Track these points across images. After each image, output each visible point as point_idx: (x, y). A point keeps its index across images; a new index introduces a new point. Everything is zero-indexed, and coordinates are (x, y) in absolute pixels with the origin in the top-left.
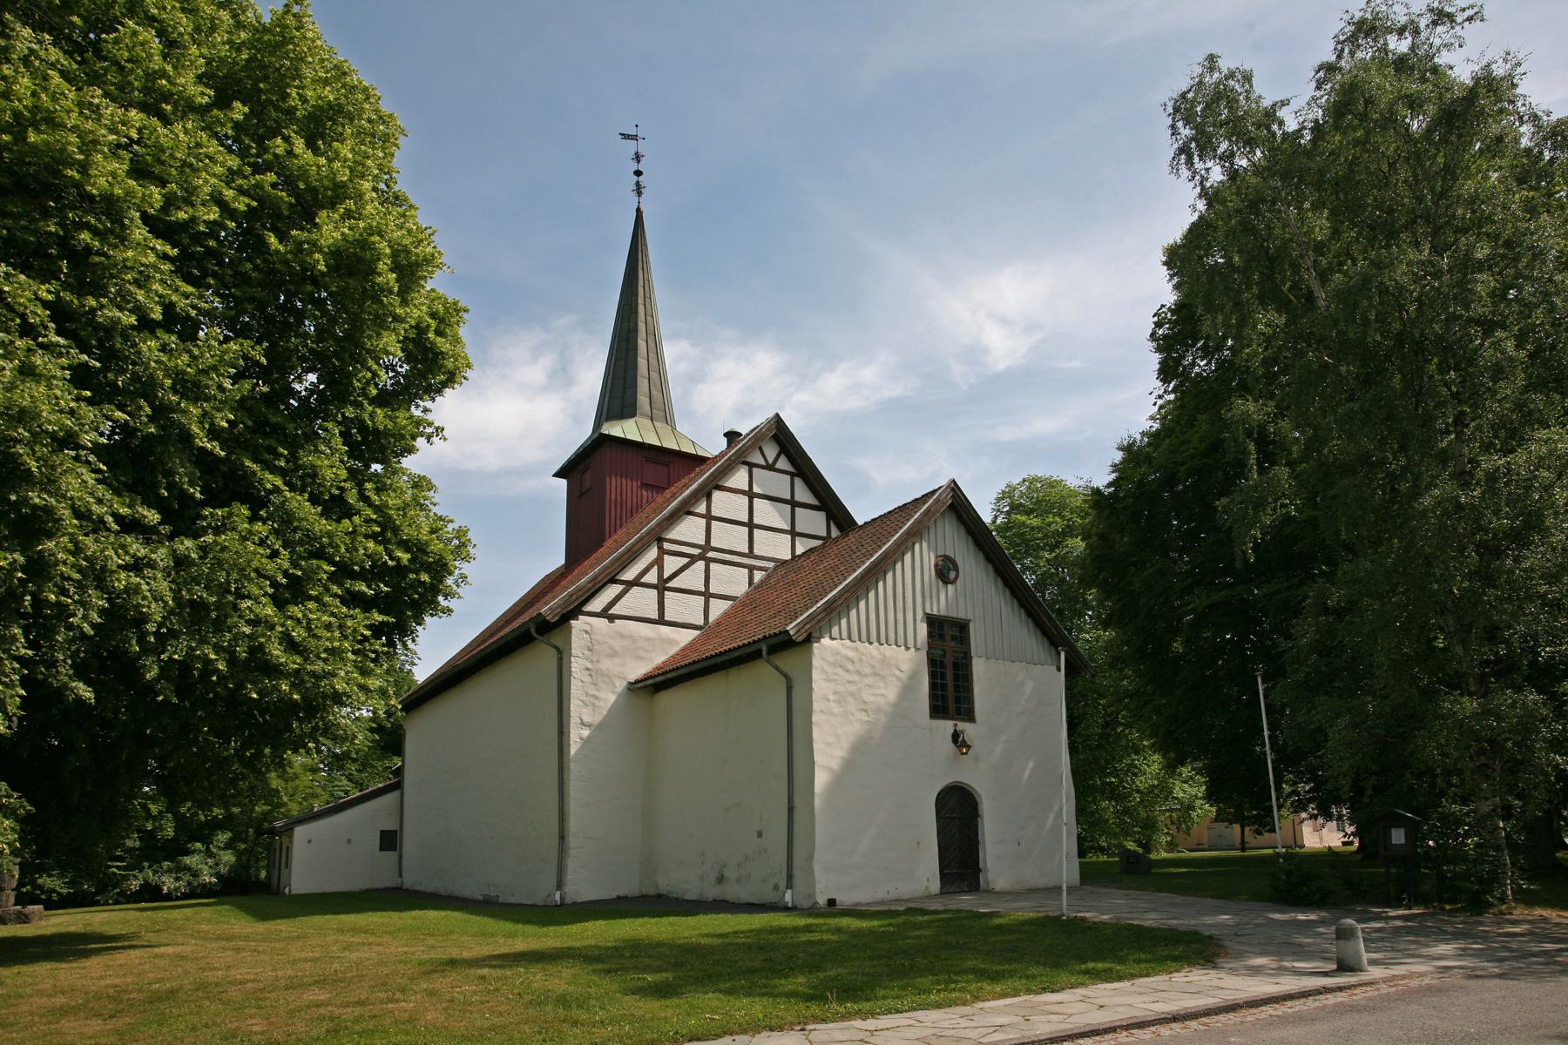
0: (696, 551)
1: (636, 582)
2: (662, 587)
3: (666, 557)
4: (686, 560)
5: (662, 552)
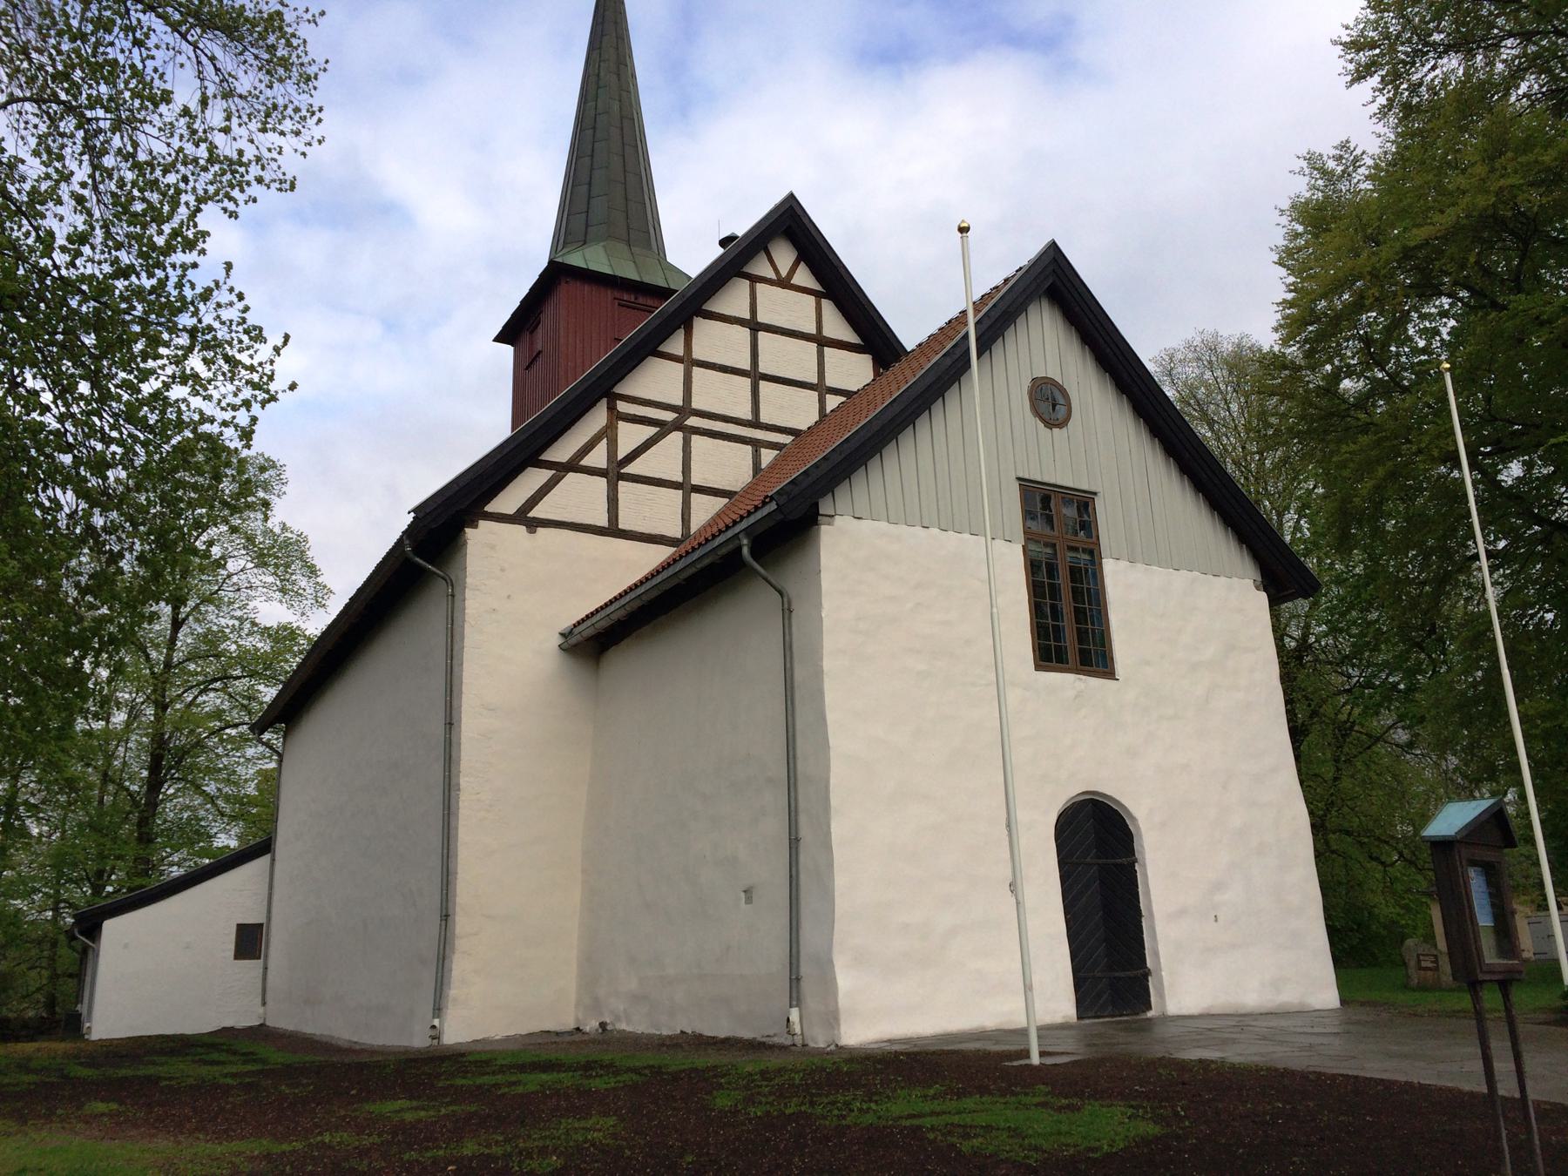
0: (669, 416)
1: (573, 466)
2: (615, 473)
3: (622, 425)
4: (651, 431)
5: (616, 416)
